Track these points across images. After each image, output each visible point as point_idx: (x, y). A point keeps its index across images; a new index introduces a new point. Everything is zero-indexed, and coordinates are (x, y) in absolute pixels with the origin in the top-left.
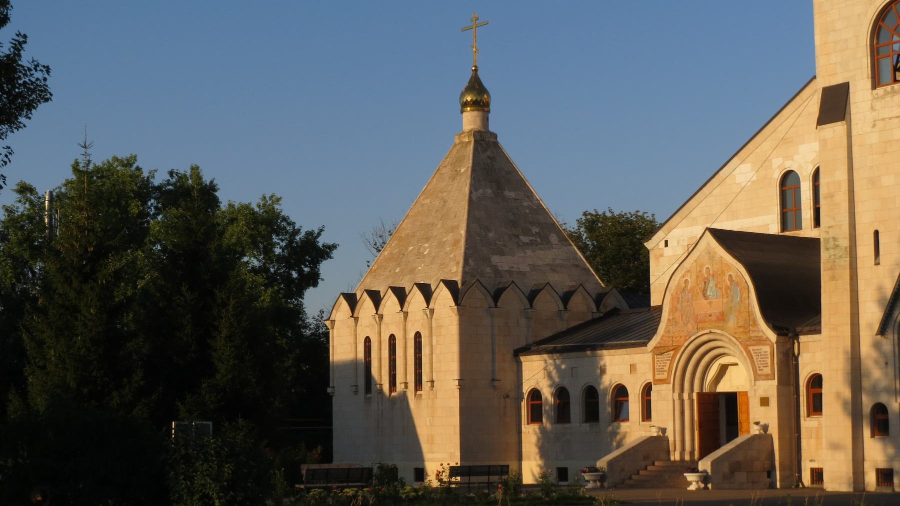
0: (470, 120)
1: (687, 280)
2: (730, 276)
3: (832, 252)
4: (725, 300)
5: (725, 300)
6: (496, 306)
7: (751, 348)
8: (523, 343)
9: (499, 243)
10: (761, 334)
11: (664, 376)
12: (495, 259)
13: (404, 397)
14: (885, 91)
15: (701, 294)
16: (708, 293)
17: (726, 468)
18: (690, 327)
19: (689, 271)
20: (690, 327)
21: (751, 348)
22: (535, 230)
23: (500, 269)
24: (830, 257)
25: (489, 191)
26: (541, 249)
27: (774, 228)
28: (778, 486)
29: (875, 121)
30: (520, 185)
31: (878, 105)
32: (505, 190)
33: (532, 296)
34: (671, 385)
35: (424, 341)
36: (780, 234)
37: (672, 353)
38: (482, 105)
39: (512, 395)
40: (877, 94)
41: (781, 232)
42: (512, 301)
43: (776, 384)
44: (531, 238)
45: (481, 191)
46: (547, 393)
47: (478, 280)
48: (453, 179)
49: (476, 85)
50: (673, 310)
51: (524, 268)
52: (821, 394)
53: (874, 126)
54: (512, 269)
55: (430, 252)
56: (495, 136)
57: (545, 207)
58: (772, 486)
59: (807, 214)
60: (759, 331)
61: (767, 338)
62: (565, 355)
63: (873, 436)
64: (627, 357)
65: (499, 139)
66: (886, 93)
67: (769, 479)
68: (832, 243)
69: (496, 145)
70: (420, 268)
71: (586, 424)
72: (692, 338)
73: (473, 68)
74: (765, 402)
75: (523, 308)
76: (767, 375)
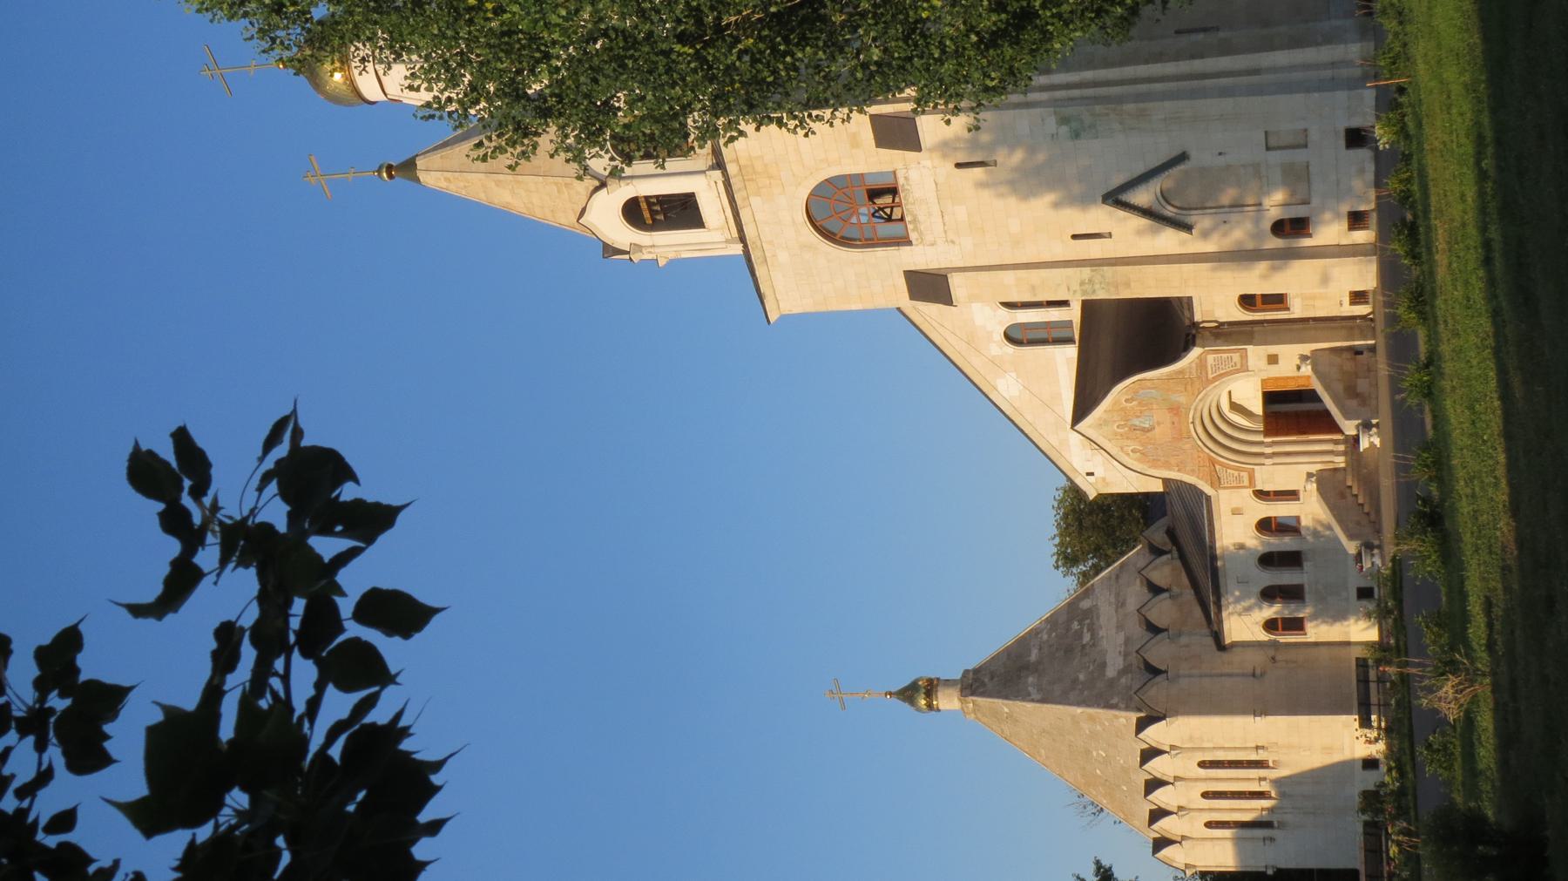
0: (948, 701)
1: (1132, 451)
2: (1126, 401)
3: (1097, 286)
4: (1155, 407)
5: (1155, 407)
6: (1166, 672)
7: (1210, 376)
8: (1210, 641)
9: (1091, 668)
10: (1194, 365)
11: (1245, 475)
12: (1111, 672)
13: (1277, 783)
14: (913, 230)
15: (1148, 434)
16: (1147, 426)
17: (1353, 403)
18: (1187, 446)
19: (1122, 448)
20: (1187, 446)
21: (1210, 376)
22: (1075, 626)
23: (1121, 667)
24: (1103, 288)
25: (1030, 679)
26: (1098, 618)
27: (1071, 351)
28: (1373, 342)
29: (947, 241)
30: (1023, 643)
31: (929, 238)
32: (1029, 661)
33: (1154, 629)
34: (1256, 467)
35: (1209, 757)
36: (1077, 345)
37: (1217, 467)
38: (931, 688)
39: (1271, 652)
40: (917, 239)
41: (1074, 343)
42: (1159, 653)
43: (1251, 346)
44: (1085, 630)
45: (1030, 689)
46: (1271, 611)
47: (1135, 693)
48: (1017, 721)
49: (908, 694)
50: (1167, 466)
51: (1121, 638)
52: (1263, 296)
53: (953, 242)
54: (1122, 653)
55: (1102, 750)
56: (966, 672)
57: (1049, 614)
58: (1372, 349)
59: (1054, 315)
60: (1190, 368)
61: (1198, 358)
62: (1222, 590)
63: (1310, 236)
64: (1223, 519)
65: (970, 668)
66: (916, 229)
67: (1365, 353)
69: (977, 671)
70: (1122, 762)
71: (1305, 568)
73: (888, 697)
74: (1273, 359)
75: (1168, 640)
76: (1241, 357)
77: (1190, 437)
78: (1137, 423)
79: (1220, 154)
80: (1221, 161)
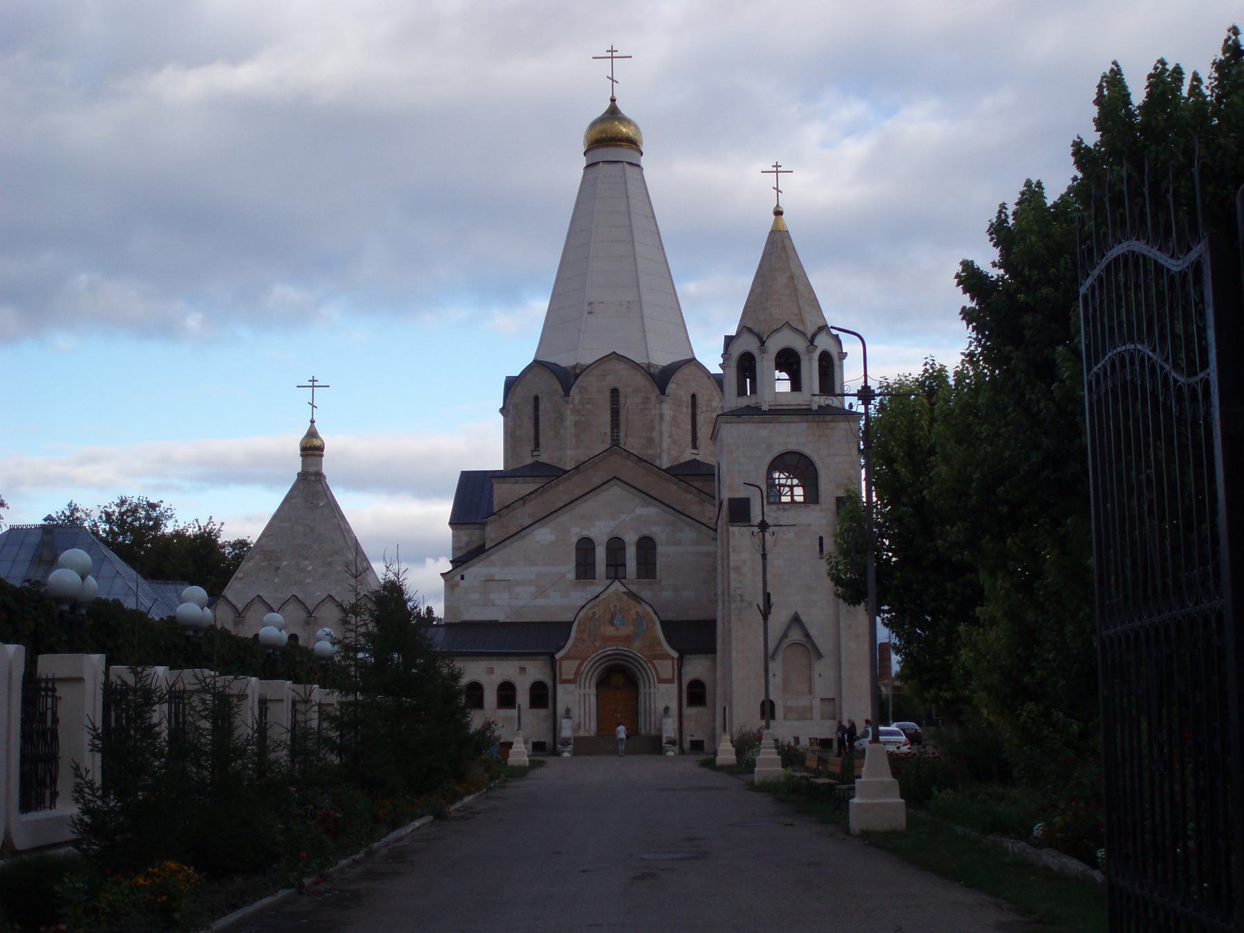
7: (654, 661)
10: (664, 652)
11: (572, 677)
16: (615, 622)
18: (597, 644)
21: (654, 661)
68: (738, 598)
72: (600, 652)
77: (606, 647)
78: (618, 616)
79: (820, 675)
80: (816, 675)
